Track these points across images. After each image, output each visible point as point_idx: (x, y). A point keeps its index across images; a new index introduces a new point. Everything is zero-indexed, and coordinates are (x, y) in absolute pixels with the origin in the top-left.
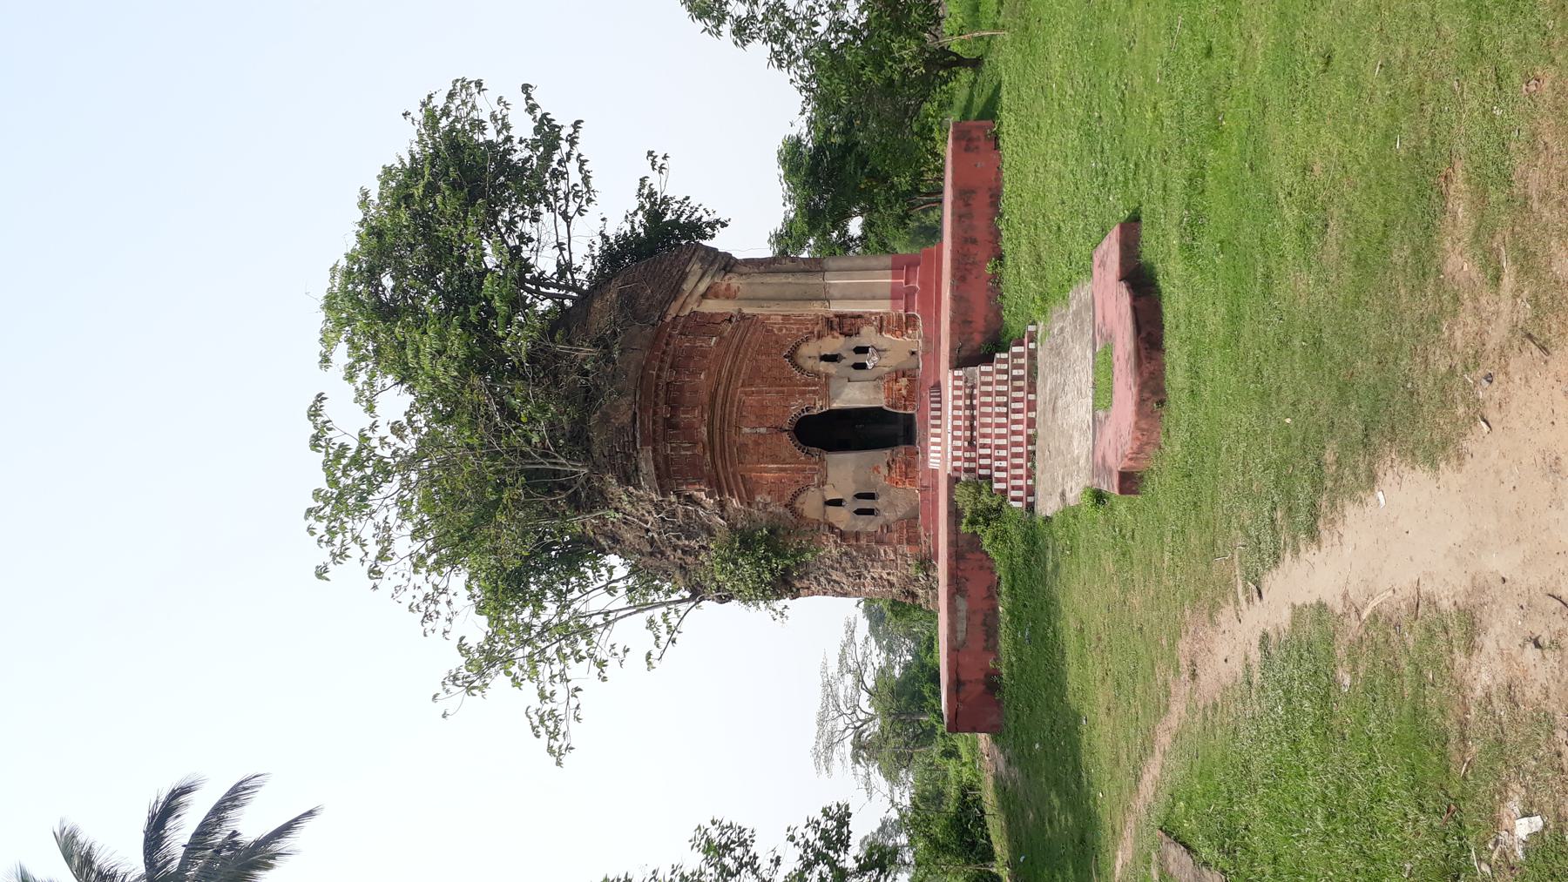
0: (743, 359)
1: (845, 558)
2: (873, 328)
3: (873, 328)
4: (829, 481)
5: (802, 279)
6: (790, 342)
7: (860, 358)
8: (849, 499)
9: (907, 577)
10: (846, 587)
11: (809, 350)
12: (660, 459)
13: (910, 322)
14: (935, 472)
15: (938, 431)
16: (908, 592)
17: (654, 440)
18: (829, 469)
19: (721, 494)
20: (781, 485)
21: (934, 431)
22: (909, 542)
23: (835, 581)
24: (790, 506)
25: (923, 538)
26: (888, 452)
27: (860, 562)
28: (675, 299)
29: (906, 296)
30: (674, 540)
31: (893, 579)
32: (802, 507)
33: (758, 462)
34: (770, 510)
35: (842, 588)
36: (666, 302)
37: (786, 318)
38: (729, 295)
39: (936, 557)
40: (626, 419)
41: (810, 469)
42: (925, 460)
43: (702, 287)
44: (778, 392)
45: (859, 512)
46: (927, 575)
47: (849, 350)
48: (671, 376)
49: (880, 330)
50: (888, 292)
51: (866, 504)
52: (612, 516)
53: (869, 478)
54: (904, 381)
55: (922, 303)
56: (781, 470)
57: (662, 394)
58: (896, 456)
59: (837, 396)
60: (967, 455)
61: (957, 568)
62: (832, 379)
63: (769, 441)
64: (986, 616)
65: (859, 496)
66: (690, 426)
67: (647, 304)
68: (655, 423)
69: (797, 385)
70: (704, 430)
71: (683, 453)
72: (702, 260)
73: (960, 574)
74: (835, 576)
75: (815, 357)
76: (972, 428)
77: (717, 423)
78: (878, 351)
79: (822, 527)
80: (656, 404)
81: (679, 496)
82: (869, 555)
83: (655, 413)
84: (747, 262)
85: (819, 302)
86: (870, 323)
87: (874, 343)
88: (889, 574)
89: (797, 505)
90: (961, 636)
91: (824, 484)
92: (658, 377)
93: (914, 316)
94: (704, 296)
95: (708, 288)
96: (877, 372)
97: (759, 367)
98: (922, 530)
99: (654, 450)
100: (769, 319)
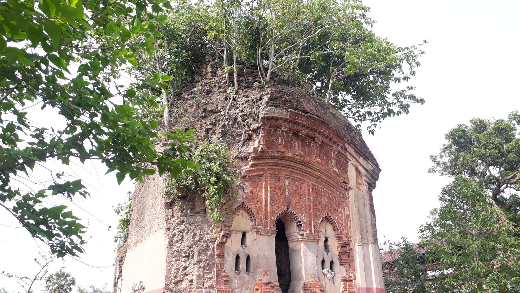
2: (345, 275)
3: (345, 275)
4: (259, 236)
5: (370, 229)
6: (335, 218)
7: (327, 265)
8: (246, 250)
10: (178, 245)
11: (329, 230)
12: (280, 122)
19: (254, 159)
23: (183, 237)
24: (243, 206)
26: (277, 283)
28: (356, 152)
31: (185, 285)
32: (240, 215)
33: (271, 187)
34: (240, 191)
35: (177, 242)
36: (355, 146)
37: (347, 217)
38: (358, 184)
40: (306, 106)
41: (267, 223)
43: (361, 168)
44: (310, 206)
45: (238, 257)
47: (332, 257)
49: (345, 280)
50: (369, 286)
56: (266, 202)
59: (308, 247)
62: (315, 244)
63: (282, 196)
65: (248, 258)
66: (291, 147)
68: (299, 124)
70: (290, 155)
71: (280, 138)
74: (188, 239)
75: (326, 234)
77: (292, 164)
78: (333, 278)
79: (226, 228)
80: (307, 128)
81: (256, 131)
83: (304, 126)
84: (371, 197)
86: (348, 273)
87: (337, 275)
88: (191, 281)
89: (242, 211)
91: (257, 232)
92: (320, 133)
94: (357, 169)
95: (359, 172)
96: (322, 276)
97: (321, 196)
99: (286, 120)
100: (346, 206)
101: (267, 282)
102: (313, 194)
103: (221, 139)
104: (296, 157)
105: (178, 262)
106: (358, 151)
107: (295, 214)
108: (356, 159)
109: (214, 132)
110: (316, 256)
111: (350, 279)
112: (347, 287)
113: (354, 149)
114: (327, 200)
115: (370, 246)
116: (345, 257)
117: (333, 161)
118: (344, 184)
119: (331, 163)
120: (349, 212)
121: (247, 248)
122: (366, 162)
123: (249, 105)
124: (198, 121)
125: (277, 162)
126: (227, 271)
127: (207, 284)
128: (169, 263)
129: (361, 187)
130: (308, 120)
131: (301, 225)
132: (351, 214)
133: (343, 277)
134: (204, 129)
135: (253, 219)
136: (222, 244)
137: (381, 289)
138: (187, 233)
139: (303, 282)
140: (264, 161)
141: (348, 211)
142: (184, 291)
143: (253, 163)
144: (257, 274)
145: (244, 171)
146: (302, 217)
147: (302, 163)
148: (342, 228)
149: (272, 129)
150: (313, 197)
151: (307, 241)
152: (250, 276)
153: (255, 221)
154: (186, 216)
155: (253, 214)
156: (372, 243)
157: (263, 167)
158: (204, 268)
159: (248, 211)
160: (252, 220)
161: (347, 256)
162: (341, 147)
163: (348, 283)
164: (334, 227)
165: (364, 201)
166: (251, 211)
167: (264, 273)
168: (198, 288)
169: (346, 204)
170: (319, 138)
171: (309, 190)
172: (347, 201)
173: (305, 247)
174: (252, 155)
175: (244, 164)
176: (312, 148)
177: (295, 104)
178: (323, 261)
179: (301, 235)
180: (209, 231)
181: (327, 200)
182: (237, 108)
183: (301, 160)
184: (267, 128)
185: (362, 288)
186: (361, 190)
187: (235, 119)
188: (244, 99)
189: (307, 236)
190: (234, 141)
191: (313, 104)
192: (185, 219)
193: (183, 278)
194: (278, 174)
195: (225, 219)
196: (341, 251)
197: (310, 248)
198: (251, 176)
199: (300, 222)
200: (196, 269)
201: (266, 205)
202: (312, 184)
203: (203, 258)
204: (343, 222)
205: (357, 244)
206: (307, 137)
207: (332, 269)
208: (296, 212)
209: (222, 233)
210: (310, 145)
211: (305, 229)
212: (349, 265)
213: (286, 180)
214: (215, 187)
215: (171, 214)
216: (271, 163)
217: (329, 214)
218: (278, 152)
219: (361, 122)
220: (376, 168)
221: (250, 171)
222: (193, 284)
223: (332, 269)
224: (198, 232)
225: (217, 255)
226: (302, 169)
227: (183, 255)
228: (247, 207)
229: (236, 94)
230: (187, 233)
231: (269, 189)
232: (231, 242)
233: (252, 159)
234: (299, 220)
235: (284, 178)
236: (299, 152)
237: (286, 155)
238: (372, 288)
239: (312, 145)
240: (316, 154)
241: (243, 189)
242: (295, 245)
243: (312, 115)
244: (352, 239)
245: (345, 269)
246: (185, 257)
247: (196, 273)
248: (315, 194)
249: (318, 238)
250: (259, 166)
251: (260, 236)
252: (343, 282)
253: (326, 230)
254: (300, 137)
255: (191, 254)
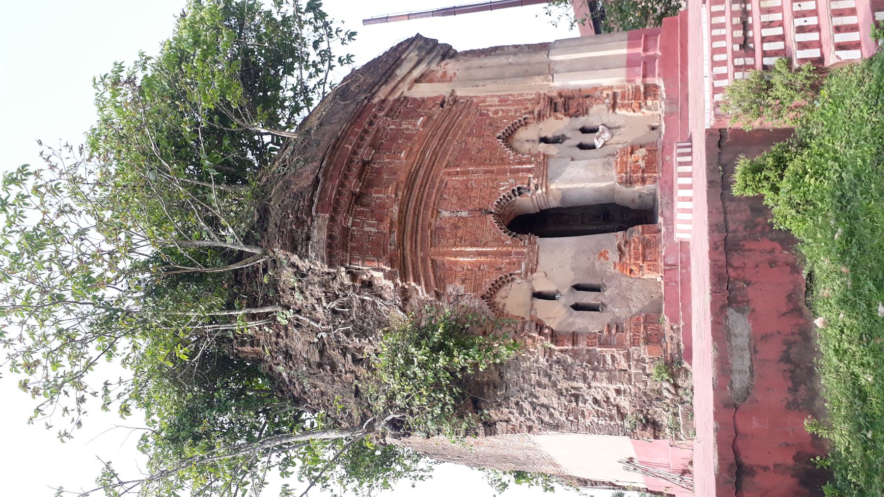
0: (451, 142)
1: (555, 366)
2: (604, 106)
3: (604, 106)
4: (539, 268)
5: (523, 58)
6: (506, 124)
7: (587, 139)
9: (645, 394)
10: (557, 414)
11: (527, 135)
12: (337, 232)
13: (650, 91)
14: (684, 246)
15: (688, 169)
16: (647, 421)
17: (334, 208)
18: (541, 254)
19: (404, 278)
20: (480, 274)
21: (681, 169)
22: (647, 341)
23: (543, 405)
24: (488, 297)
25: (668, 333)
26: (620, 234)
27: (577, 370)
28: (386, 82)
29: (645, 63)
30: (343, 337)
31: (624, 403)
32: (503, 301)
33: (455, 245)
35: (551, 415)
36: (377, 84)
37: (503, 101)
38: (444, 78)
39: (688, 354)
40: (306, 182)
41: (517, 253)
42: (671, 233)
43: (416, 73)
44: (486, 172)
45: (577, 307)
46: (676, 386)
47: (574, 130)
48: (369, 154)
49: (614, 106)
50: (624, 62)
51: (588, 298)
52: (283, 317)
53: (594, 265)
54: (642, 152)
55: (663, 66)
56: (480, 254)
57: (355, 170)
58: (631, 233)
59: (557, 175)
60: (740, 61)
61: (728, 264)
62: (551, 162)
63: (470, 224)
64: (789, 344)
65: (578, 287)
66: (382, 206)
67: (357, 90)
68: (339, 193)
69: (509, 164)
70: (396, 209)
71: (367, 229)
72: (420, 48)
73: (732, 273)
74: (545, 396)
75: (533, 141)
76: (745, 26)
77: (412, 205)
78: (609, 128)
79: (527, 327)
80: (346, 177)
81: (354, 276)
82: (589, 362)
83: (342, 184)
84: (466, 53)
85: (541, 77)
86: (599, 100)
87: (605, 121)
88: (618, 392)
90: (740, 381)
91: (533, 271)
92: (354, 153)
93: (656, 87)
94: (417, 81)
96: (607, 150)
97: (468, 150)
98: (666, 324)
99: (332, 219)
100: (484, 101)
101: (617, 253)
102: (465, 165)
103: (371, 338)
104: (400, 198)
105: (586, 413)
106: (384, 79)
107: (501, 199)
108: (400, 82)
109: (360, 350)
110: (573, 160)
111: (611, 96)
112: (626, 102)
113: (382, 85)
114: (474, 139)
115: (555, 57)
116: (573, 105)
117: (404, 126)
118: (445, 105)
119: (408, 129)
120: (493, 96)
121: (559, 290)
122: (405, 63)
123: (307, 288)
124: (340, 376)
125: (409, 233)
126: (600, 328)
127: (624, 365)
128: (589, 430)
129: (450, 73)
130: (332, 176)
131: (519, 188)
132: (498, 94)
133: (609, 110)
134: (353, 368)
135: (510, 278)
136: (555, 337)
137: (629, 39)
138: (537, 398)
139: (618, 185)
140: (409, 259)
141: (493, 99)
142: (636, 407)
143: (411, 279)
144: (605, 271)
145: (426, 295)
146: (505, 187)
147: (410, 186)
148: (523, 111)
149: (350, 244)
150: (471, 165)
151: (547, 176)
152: (607, 285)
153: (514, 274)
154: (506, 398)
155: (501, 278)
156: (548, 55)
157: (420, 260)
158: (595, 369)
159: (496, 288)
160: (513, 280)
161: (571, 101)
162: (379, 110)
163: (619, 101)
164: (522, 125)
165: (475, 68)
166: (496, 281)
167: (602, 258)
168: (630, 380)
169: (481, 102)
170: (364, 153)
171: (457, 173)
172: (475, 100)
173: (557, 181)
174: (399, 281)
175: (414, 295)
176: (382, 167)
177: (302, 203)
178: (582, 147)
179: (537, 189)
180: (532, 359)
181: (474, 139)
182: (314, 309)
183: (405, 188)
184: (348, 255)
185: (628, 75)
186: (455, 73)
187: (334, 312)
188: (297, 295)
189: (538, 178)
190: (375, 314)
191: (301, 168)
192: (513, 399)
193: (613, 406)
194: (431, 232)
195: (511, 329)
196: (563, 112)
197: (558, 171)
198: (436, 283)
199: (513, 191)
200: (598, 384)
201: (485, 254)
202: (446, 167)
203: (578, 372)
204: (512, 108)
205: (552, 84)
206: (363, 176)
207: (594, 131)
208: (496, 198)
209: (535, 335)
210: (377, 169)
211: (526, 181)
212: (588, 97)
213: (441, 216)
214: (455, 353)
215: (504, 424)
216: (411, 245)
217: (498, 134)
218: (391, 232)
219: (334, 56)
220: (415, 43)
221: (426, 285)
222: (622, 388)
223: (594, 131)
224: (534, 378)
225: (573, 345)
226: (421, 185)
227: (574, 404)
228: (490, 289)
229: (288, 308)
230: (537, 398)
231: (458, 249)
232: (552, 320)
233: (406, 282)
234: (510, 192)
235: (438, 219)
236: (391, 193)
237: (396, 217)
238: (628, 55)
239: (376, 166)
240: (394, 158)
241: (458, 297)
242: (554, 198)
243: (322, 170)
244: (542, 92)
245: (595, 106)
246: (577, 402)
247: (605, 384)
248: (464, 162)
249: (542, 158)
250: (418, 267)
251: (538, 266)
252: (617, 110)
253: (527, 141)
254: (364, 191)
255: (573, 392)
